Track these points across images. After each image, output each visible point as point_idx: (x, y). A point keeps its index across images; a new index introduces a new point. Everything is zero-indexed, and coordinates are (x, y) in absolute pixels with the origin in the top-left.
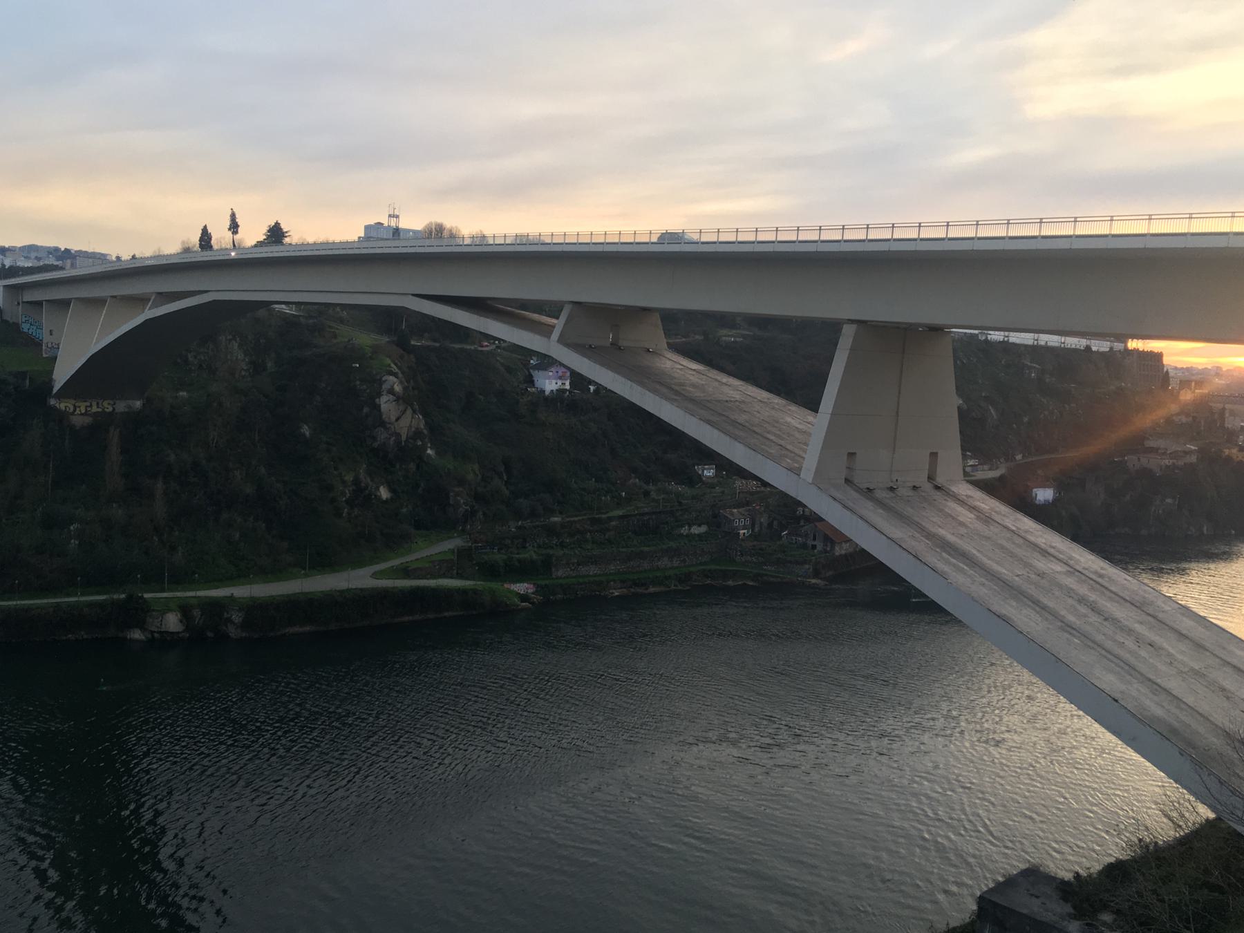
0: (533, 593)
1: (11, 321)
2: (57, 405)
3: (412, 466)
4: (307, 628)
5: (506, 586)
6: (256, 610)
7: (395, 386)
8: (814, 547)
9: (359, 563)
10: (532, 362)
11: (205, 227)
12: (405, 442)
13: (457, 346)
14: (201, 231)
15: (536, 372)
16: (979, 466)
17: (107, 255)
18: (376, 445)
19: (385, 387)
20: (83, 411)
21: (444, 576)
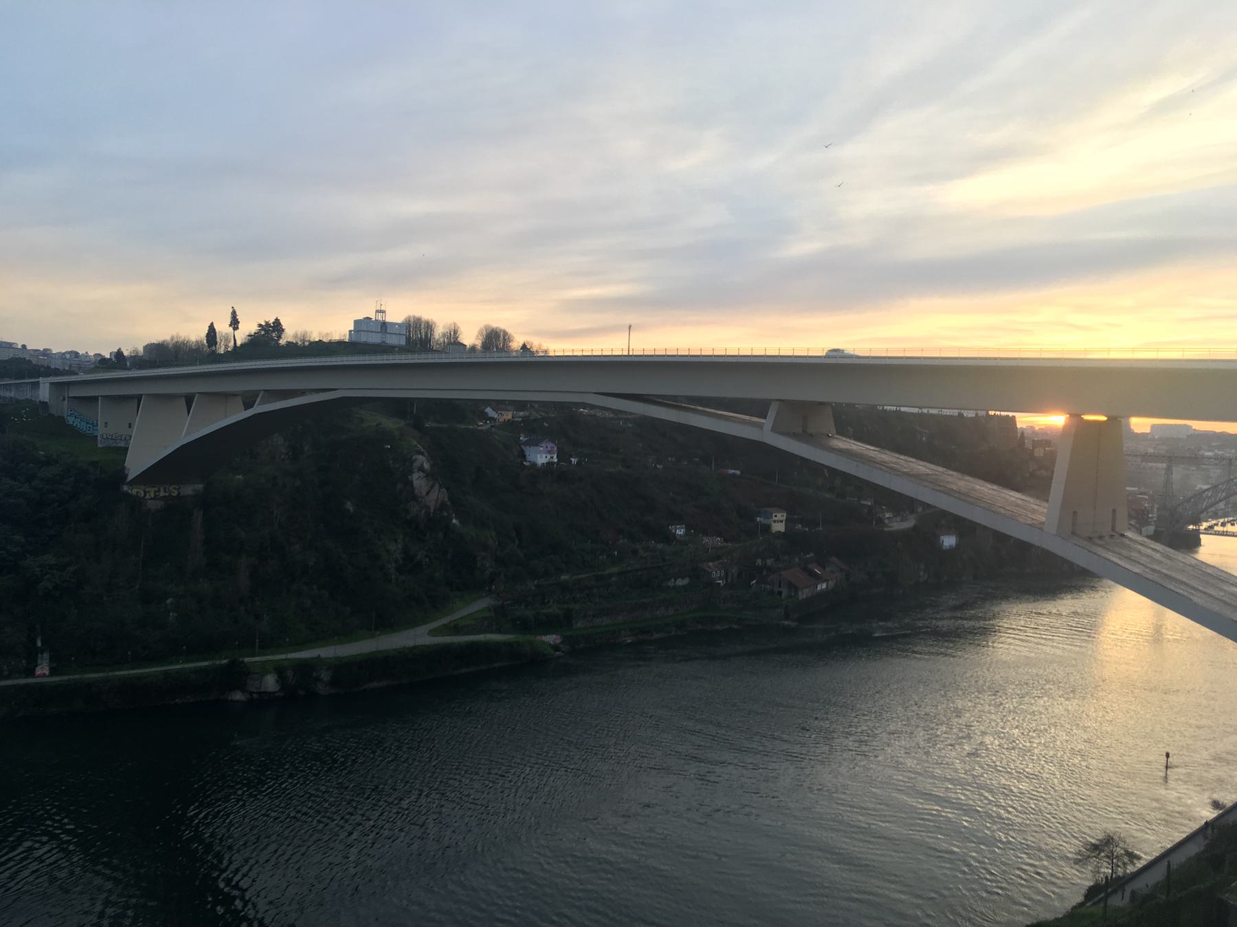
0: (560, 643)
1: (56, 415)
2: (130, 491)
3: (441, 535)
4: (384, 683)
5: (538, 638)
6: (345, 671)
7: (425, 464)
8: (780, 593)
9: (413, 623)
10: (521, 438)
11: (212, 324)
12: (433, 513)
13: (463, 426)
14: (207, 328)
15: (528, 447)
16: (894, 519)
17: (13, 343)
18: (409, 517)
19: (416, 465)
20: (152, 496)
21: (485, 632)
